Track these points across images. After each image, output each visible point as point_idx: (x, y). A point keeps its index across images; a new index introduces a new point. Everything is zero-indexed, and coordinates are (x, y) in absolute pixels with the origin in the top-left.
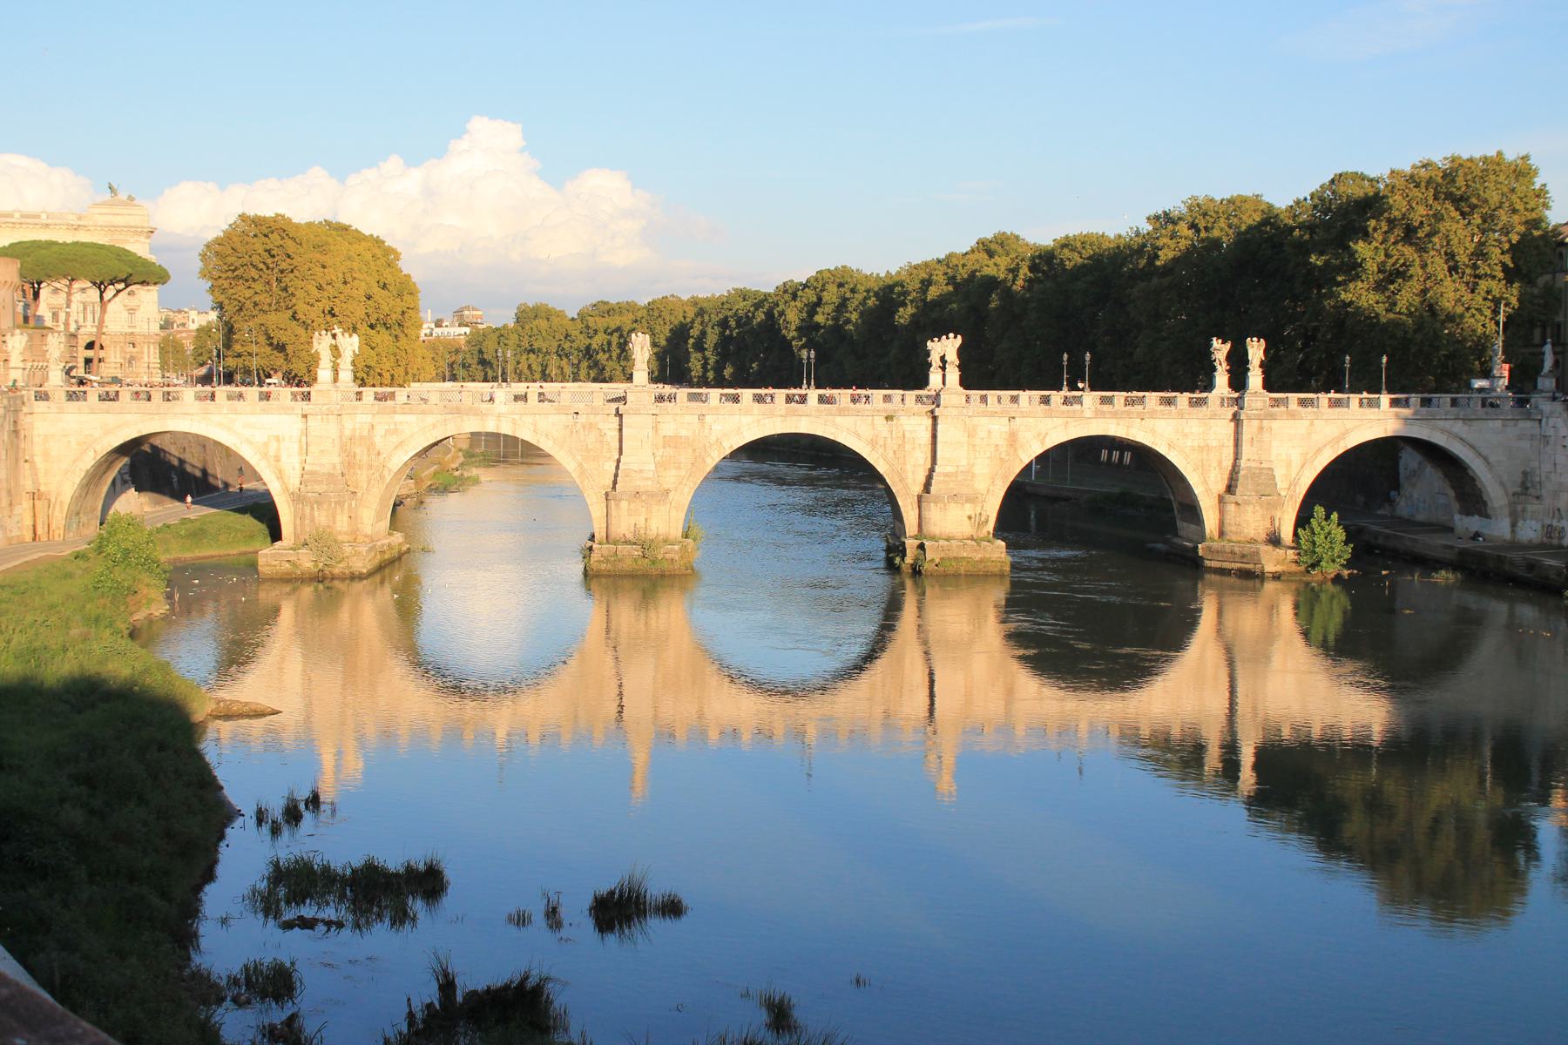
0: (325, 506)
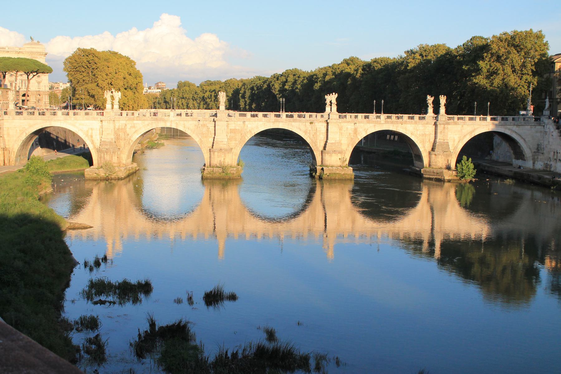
0: (109, 153)
